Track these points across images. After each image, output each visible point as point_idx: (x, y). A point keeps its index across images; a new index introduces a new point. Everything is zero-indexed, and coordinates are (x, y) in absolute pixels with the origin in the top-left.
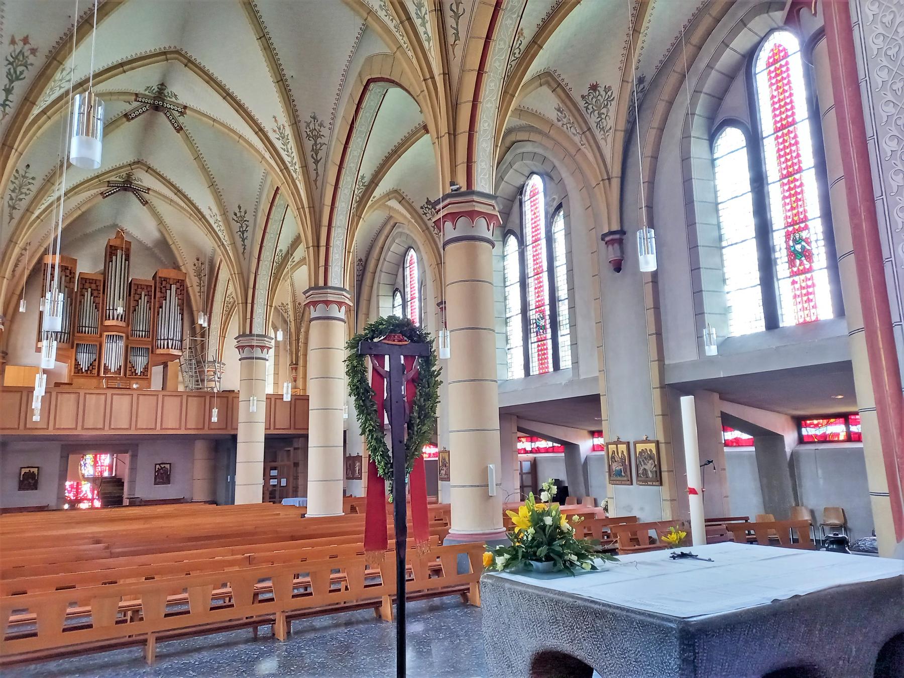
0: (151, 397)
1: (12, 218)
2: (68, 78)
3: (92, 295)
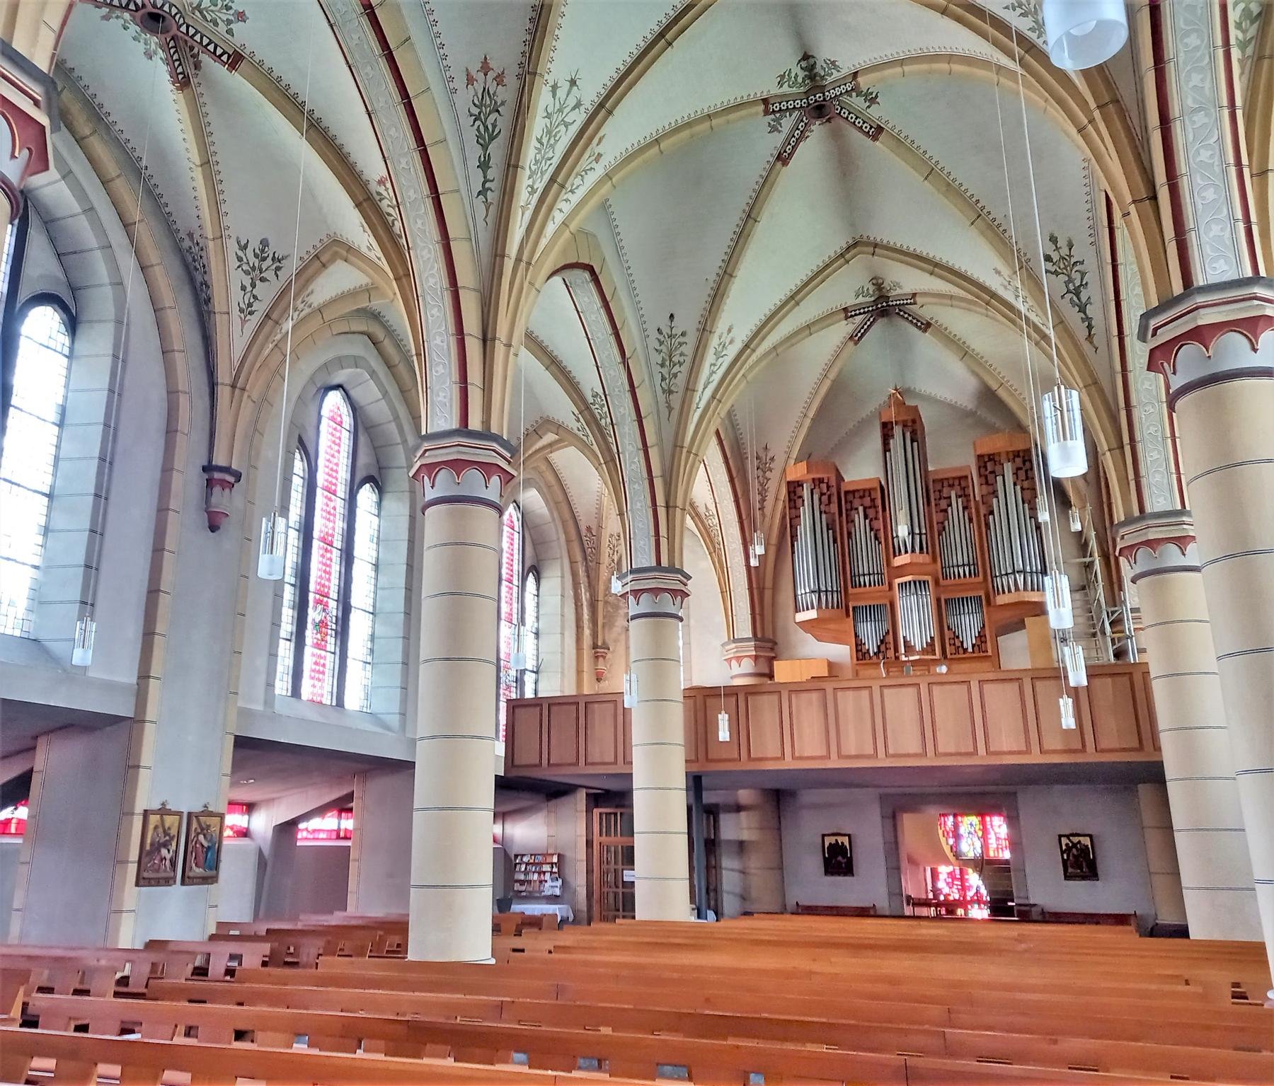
0: (955, 687)
1: (670, 409)
2: (572, 102)
3: (866, 517)
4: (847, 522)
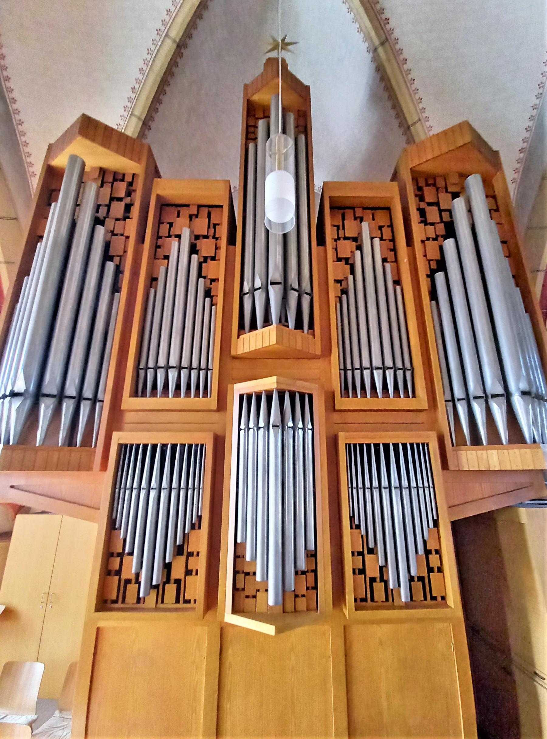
3: (193, 250)
4: (154, 256)
